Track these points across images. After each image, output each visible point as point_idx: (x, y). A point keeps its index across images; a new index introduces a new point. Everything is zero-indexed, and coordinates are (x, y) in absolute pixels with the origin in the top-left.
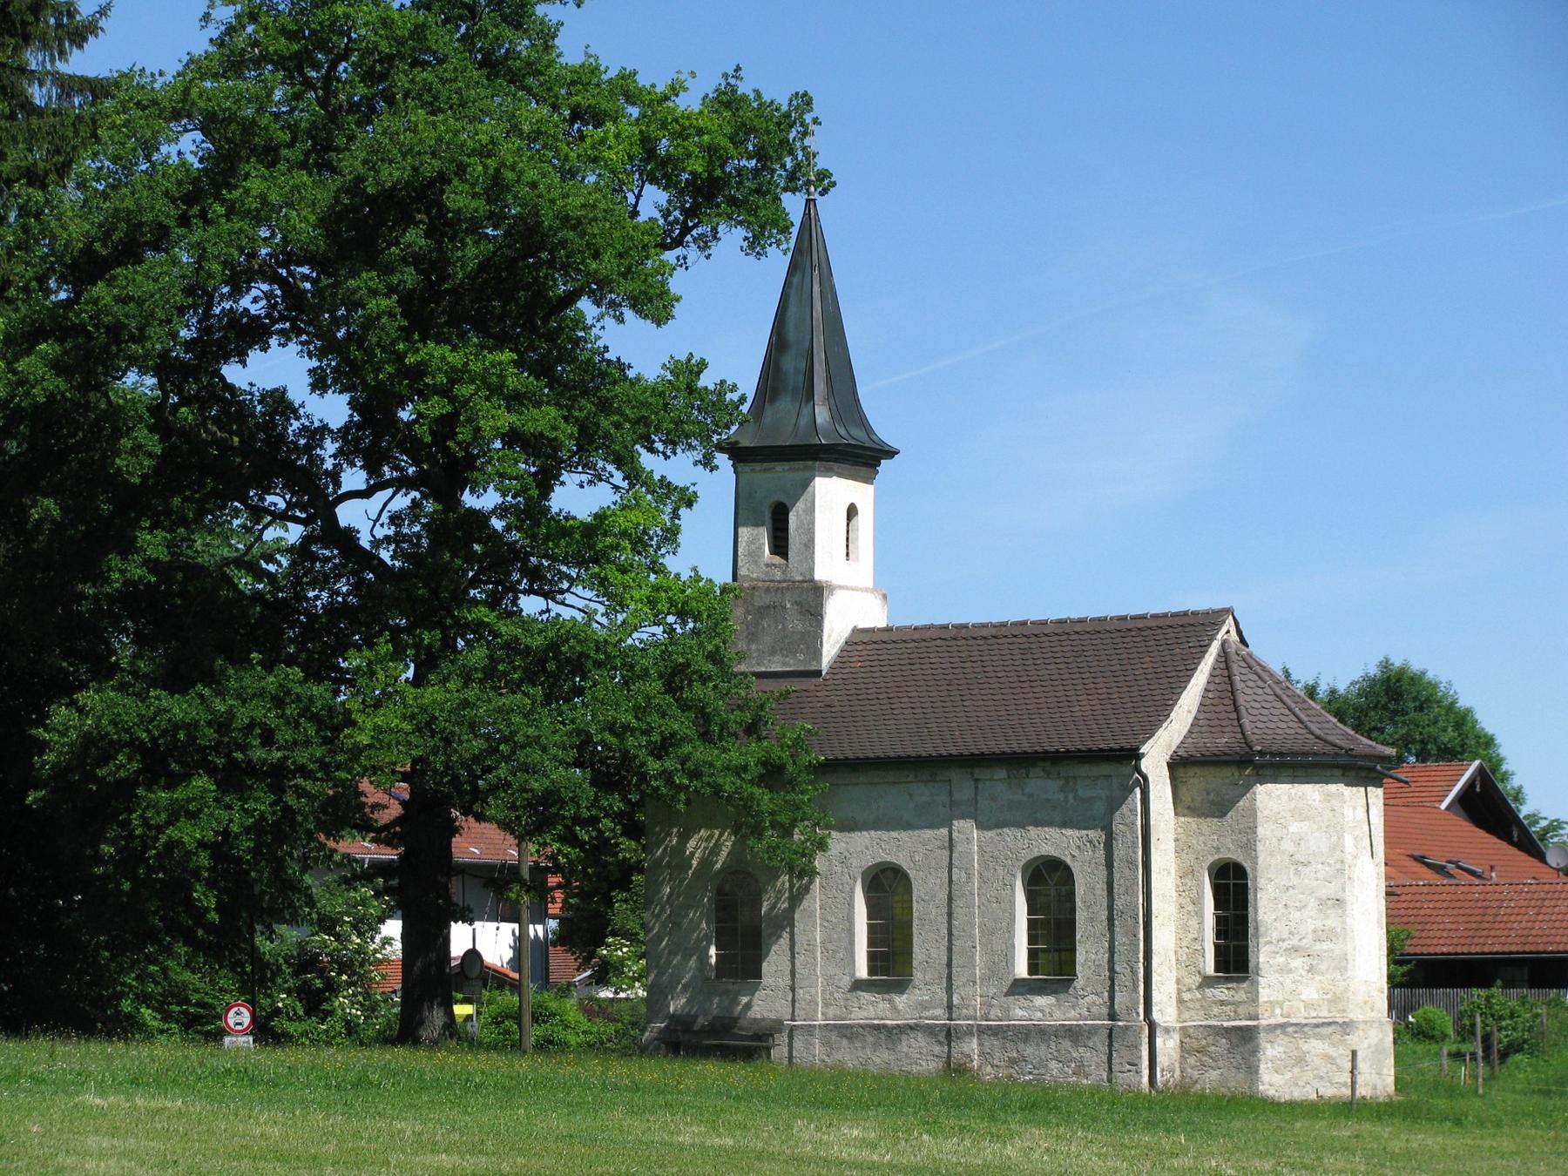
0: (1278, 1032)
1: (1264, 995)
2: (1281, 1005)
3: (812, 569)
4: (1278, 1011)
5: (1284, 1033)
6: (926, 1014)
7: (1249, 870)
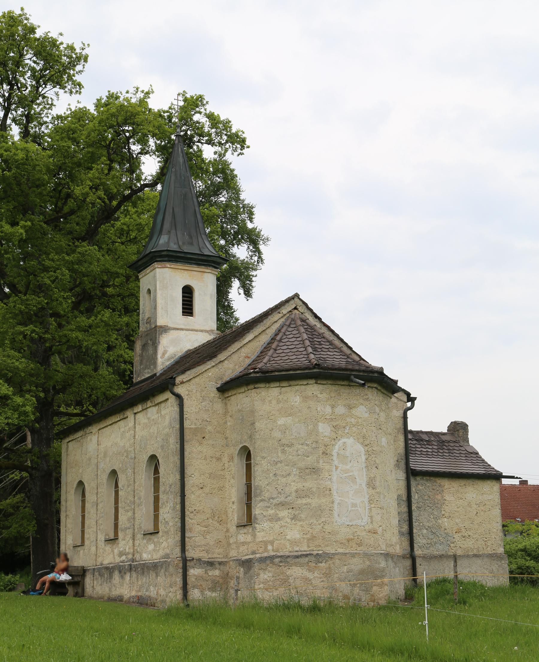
0: (268, 562)
2: (272, 543)
4: (270, 547)
5: (272, 563)
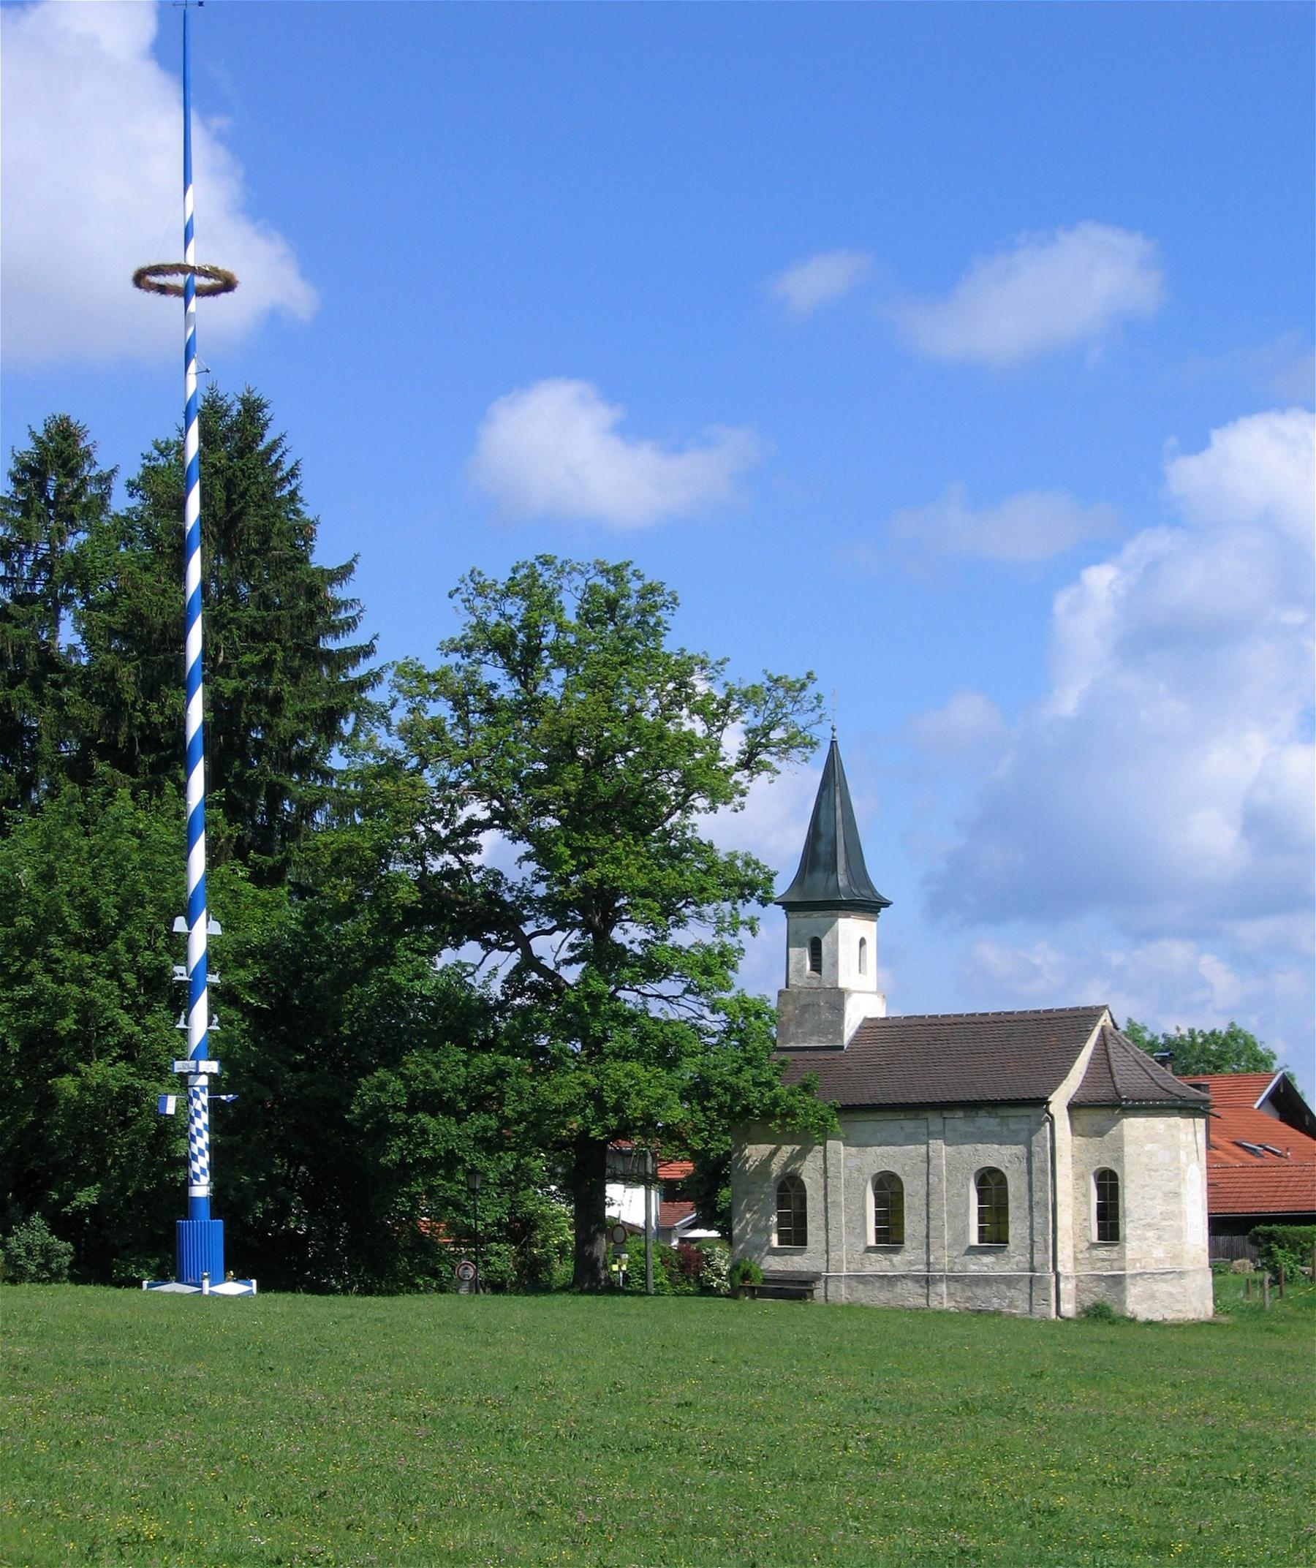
1: (1129, 1254)
2: (1139, 1260)
3: (837, 981)
4: (1138, 1265)
6: (913, 1268)
7: (1119, 1175)
